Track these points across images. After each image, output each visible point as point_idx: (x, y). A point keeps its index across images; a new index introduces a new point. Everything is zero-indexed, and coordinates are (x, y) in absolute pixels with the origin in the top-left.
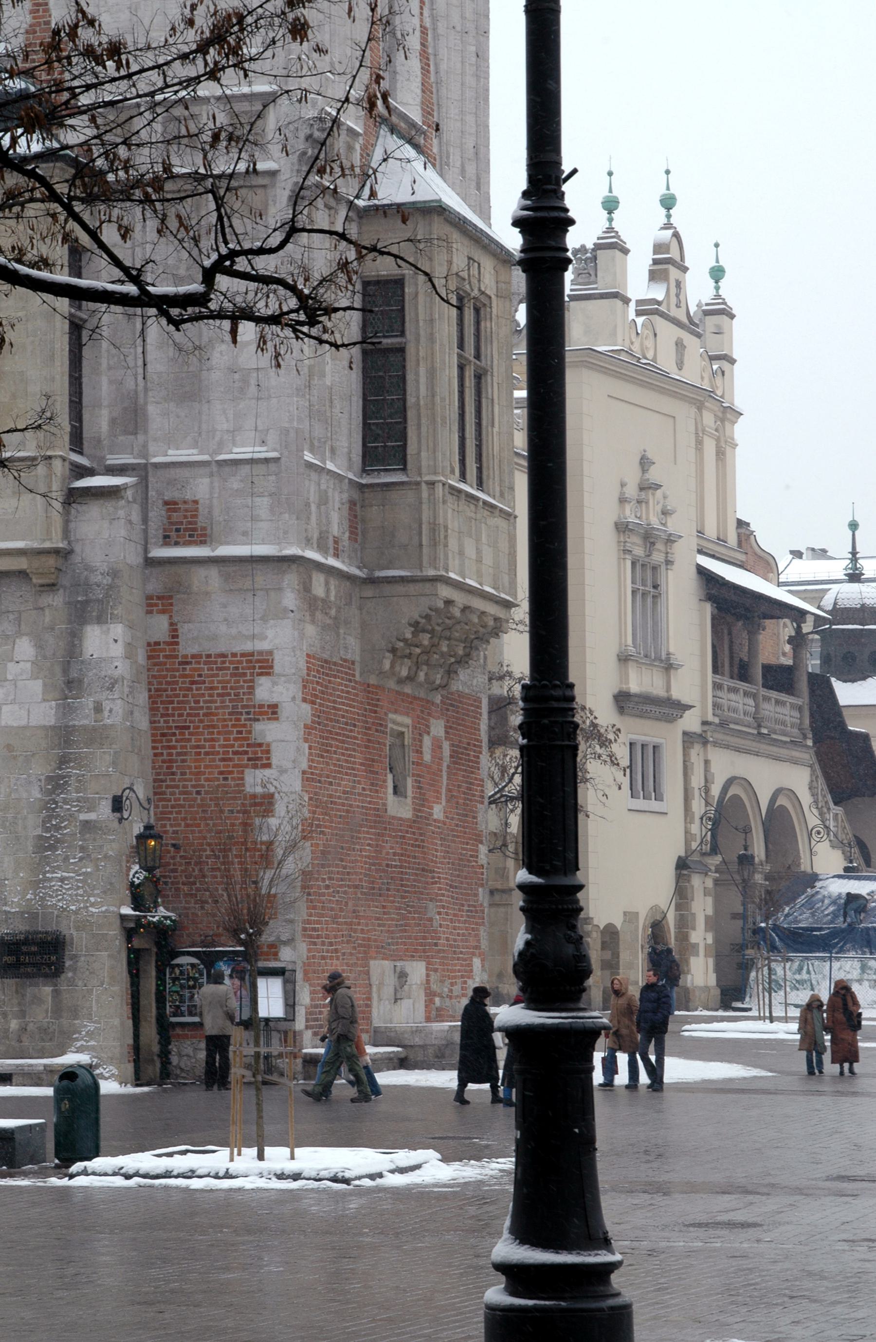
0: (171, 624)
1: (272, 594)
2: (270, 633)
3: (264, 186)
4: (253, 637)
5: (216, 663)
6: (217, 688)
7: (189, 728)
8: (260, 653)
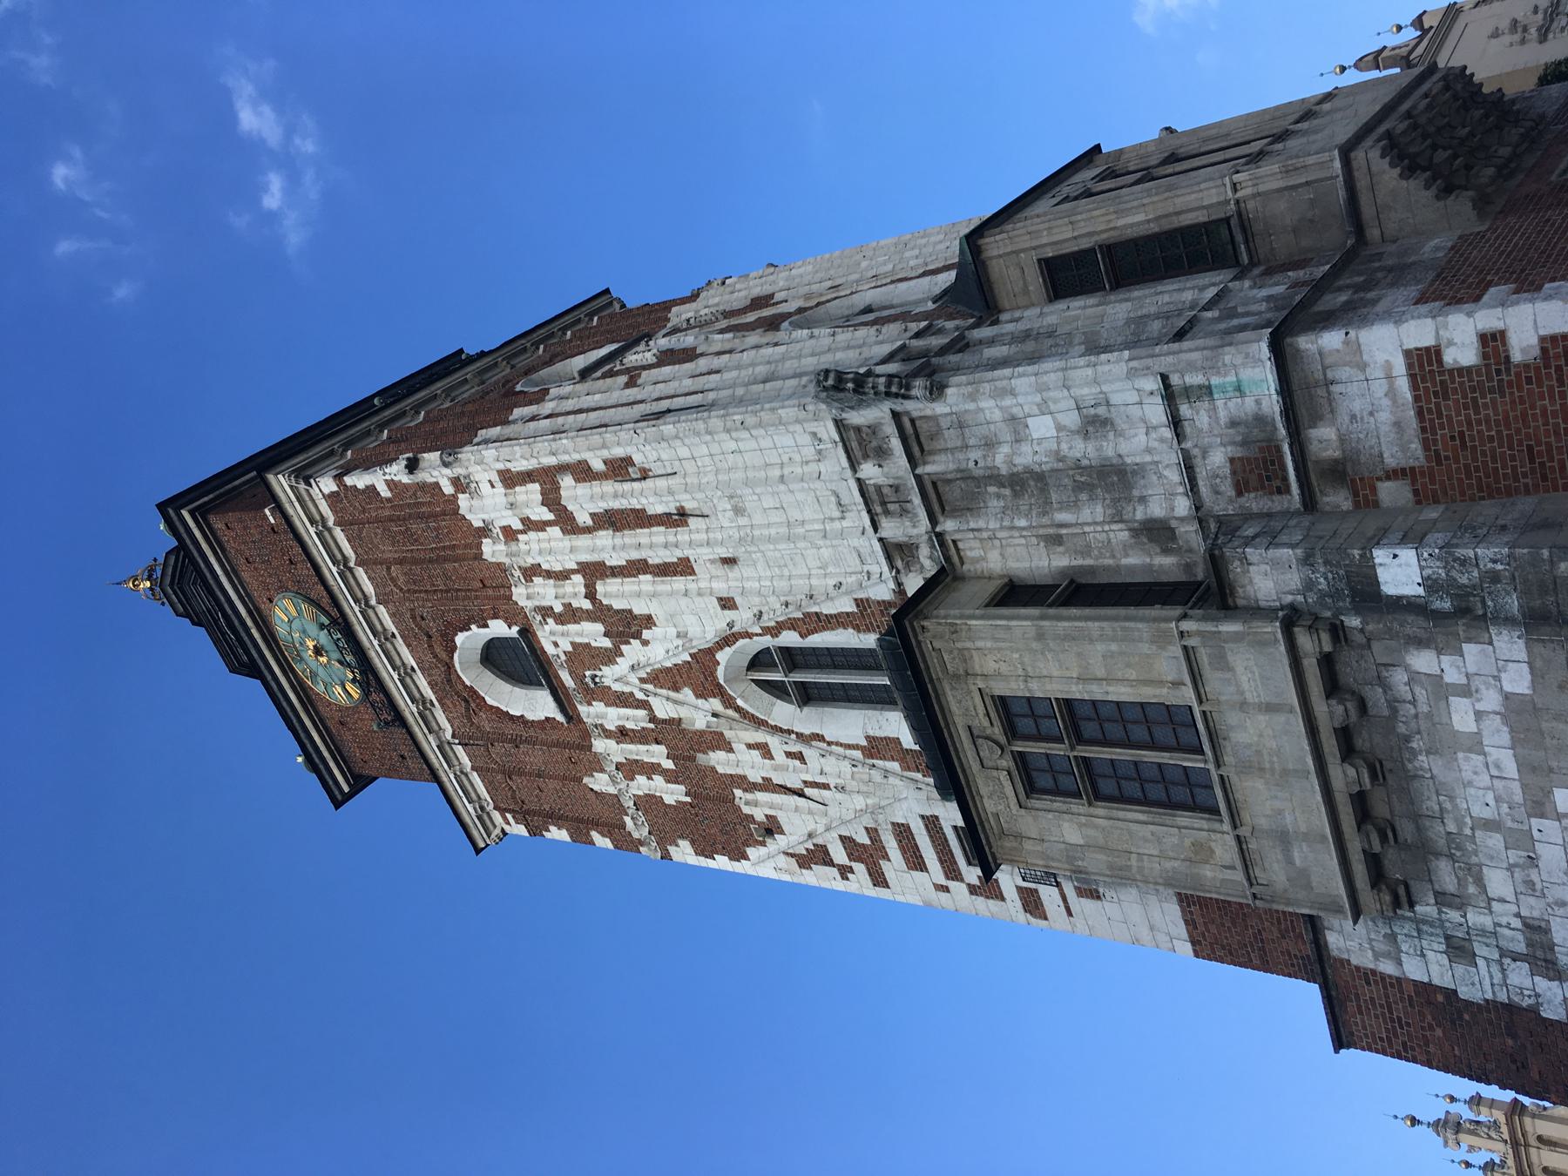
0: (1388, 478)
1: (1328, 361)
2: (1380, 357)
3: (913, 421)
4: (1389, 377)
5: (1432, 420)
6: (1468, 417)
7: (1530, 448)
8: (1409, 366)
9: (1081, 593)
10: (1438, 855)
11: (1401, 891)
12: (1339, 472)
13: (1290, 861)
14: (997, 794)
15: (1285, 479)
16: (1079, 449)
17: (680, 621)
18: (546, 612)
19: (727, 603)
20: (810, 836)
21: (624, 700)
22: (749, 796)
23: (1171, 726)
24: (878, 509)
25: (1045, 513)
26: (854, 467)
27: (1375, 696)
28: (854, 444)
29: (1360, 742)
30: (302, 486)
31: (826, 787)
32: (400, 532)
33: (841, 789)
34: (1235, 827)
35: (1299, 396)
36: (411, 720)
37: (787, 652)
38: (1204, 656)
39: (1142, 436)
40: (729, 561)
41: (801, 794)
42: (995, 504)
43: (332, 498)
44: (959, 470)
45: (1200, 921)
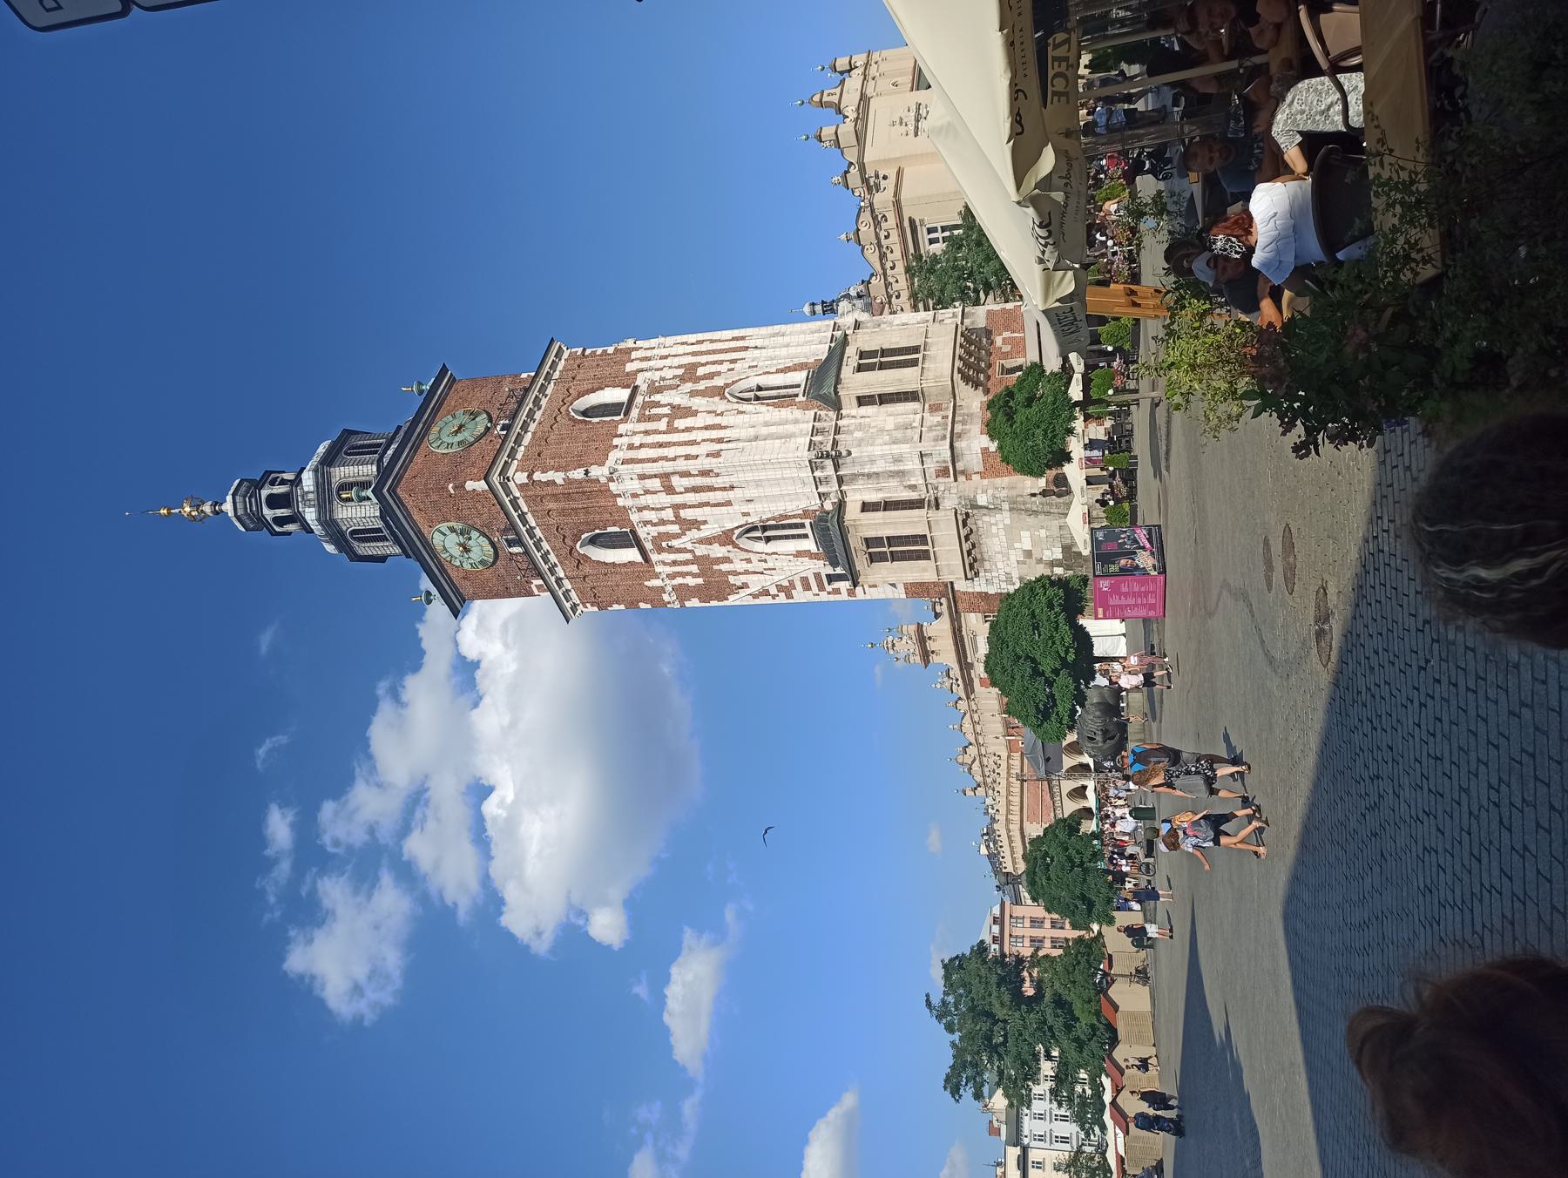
9: (889, 506)
12: (963, 472)
14: (861, 562)
18: (646, 523)
19: (745, 514)
21: (679, 551)
23: (922, 539)
39: (913, 464)
43: (521, 487)
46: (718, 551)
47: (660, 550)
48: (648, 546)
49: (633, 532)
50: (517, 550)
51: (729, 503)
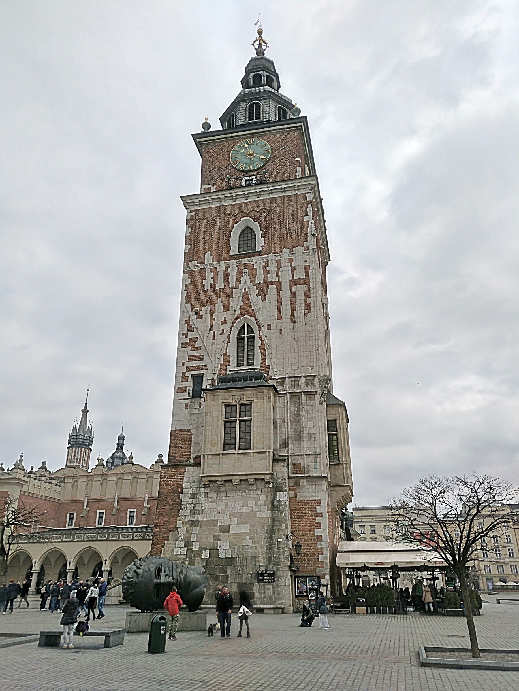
10: (217, 494)
11: (207, 486)
12: (297, 484)
13: (214, 464)
15: (296, 474)
16: (305, 432)
17: (265, 310)
18: (267, 263)
19: (269, 327)
20: (197, 328)
22: (208, 312)
24: (293, 379)
25: (290, 420)
26: (305, 377)
27: (254, 487)
28: (310, 378)
29: (243, 482)
30: (310, 188)
31: (214, 339)
32: (293, 218)
33: (213, 344)
34: (222, 454)
35: (314, 479)
36: (230, 192)
37: (253, 337)
38: (264, 455)
39: (306, 447)
40: (281, 331)
41: (211, 330)
42: (293, 408)
44: (302, 403)
45: (182, 433)
46: (236, 304)
47: (241, 268)
48: (245, 261)
49: (260, 253)
50: (244, 183)
51: (279, 317)
